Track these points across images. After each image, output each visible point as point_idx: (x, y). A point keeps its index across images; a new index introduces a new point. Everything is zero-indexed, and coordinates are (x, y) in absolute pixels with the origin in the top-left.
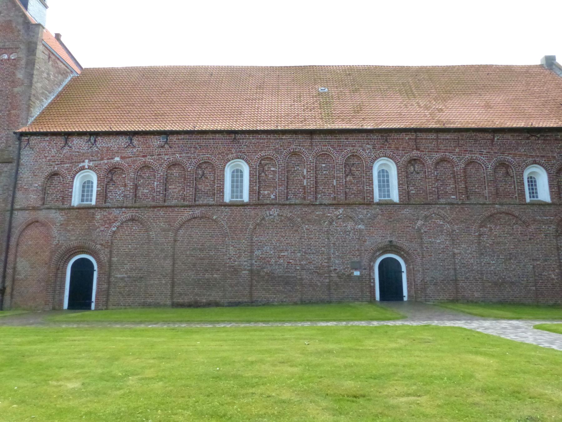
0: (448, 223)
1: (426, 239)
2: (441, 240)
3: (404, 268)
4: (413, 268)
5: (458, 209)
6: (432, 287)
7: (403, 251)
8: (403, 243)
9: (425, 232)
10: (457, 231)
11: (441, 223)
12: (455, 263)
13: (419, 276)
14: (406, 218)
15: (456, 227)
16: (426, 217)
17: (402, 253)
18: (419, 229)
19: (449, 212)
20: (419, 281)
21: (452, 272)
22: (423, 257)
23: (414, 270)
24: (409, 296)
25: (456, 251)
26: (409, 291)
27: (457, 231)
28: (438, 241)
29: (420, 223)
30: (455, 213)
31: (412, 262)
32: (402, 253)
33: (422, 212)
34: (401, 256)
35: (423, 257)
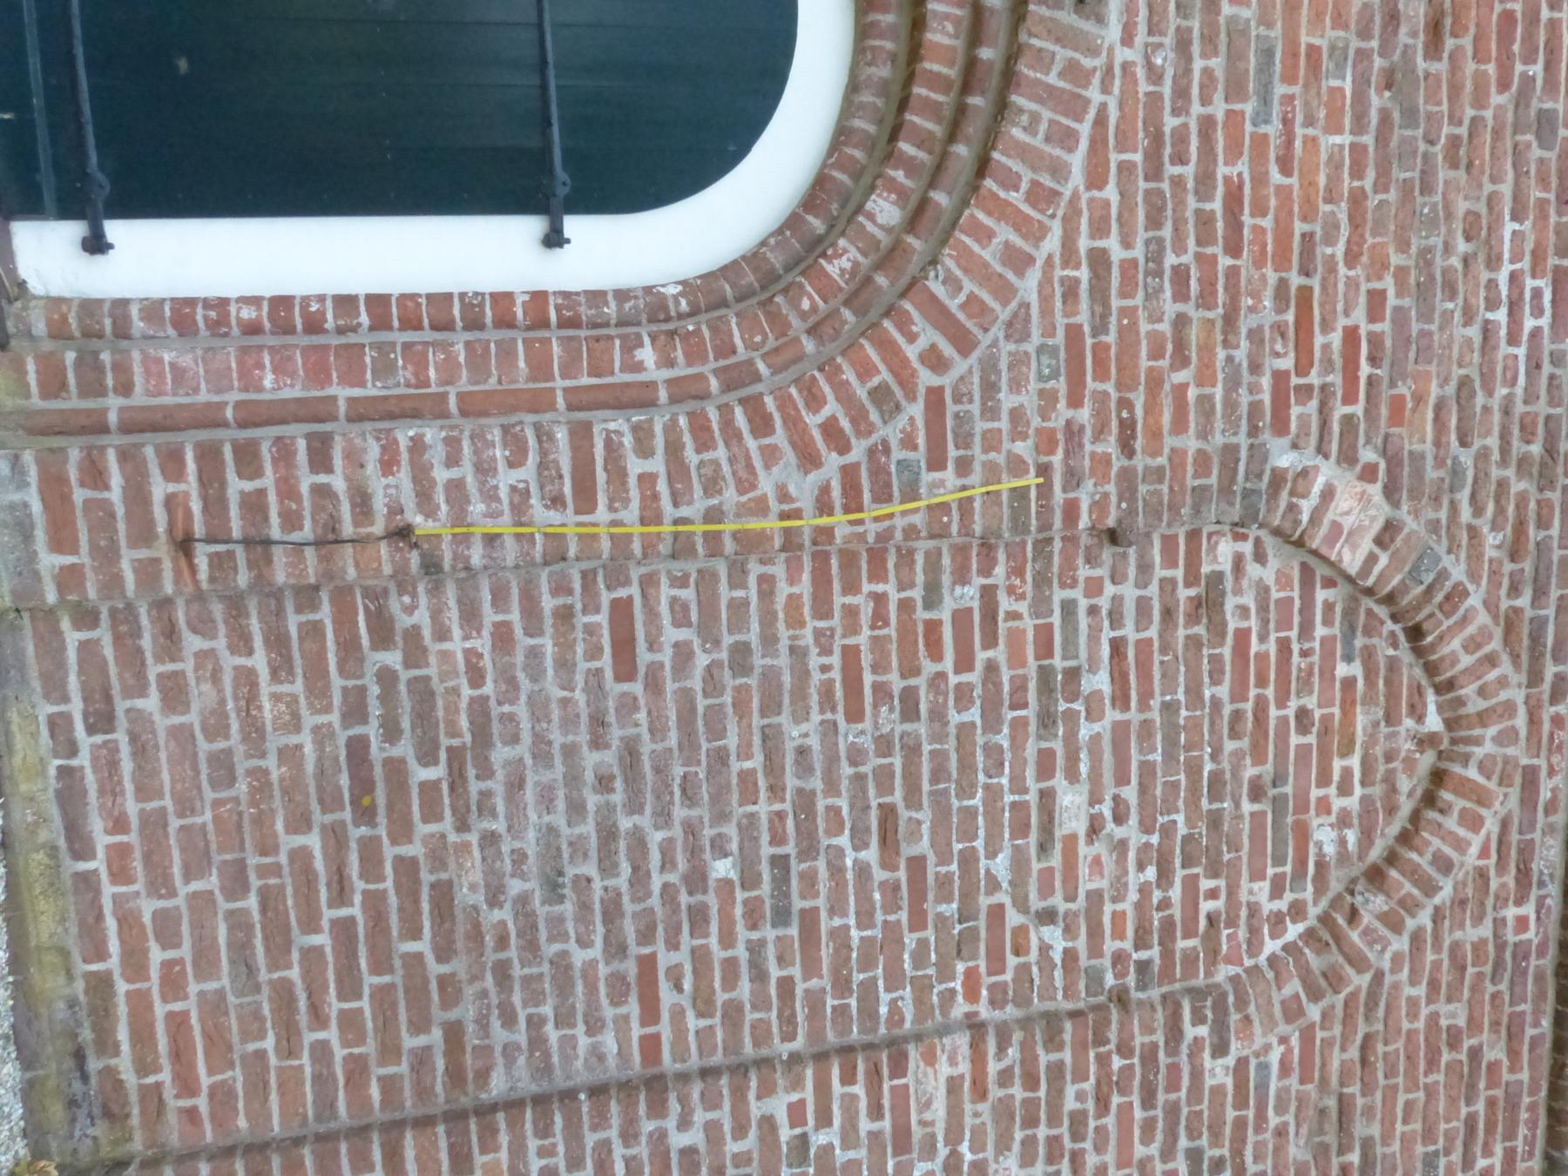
0: (1326, 934)
1: (1118, 597)
2: (1087, 848)
3: (619, 251)
4: (638, 398)
5: (1495, 1052)
6: (314, 735)
7: (918, 214)
8: (1054, 223)
9: (1209, 604)
10: (1218, 1072)
11: (1324, 836)
12: (743, 1071)
13: (494, 492)
14: (1427, 286)
15: (1268, 1044)
16: (1411, 619)
17: (885, 211)
18: (1260, 506)
19: (1472, 933)
20: (391, 490)
21: (605, 1045)
22: (833, 564)
23: (579, 401)
24: (99, 326)
25: (931, 1080)
26: (182, 316)
27: (1218, 1072)
28: (1072, 802)
29: (1351, 509)
30: (1454, 1014)
31: (738, 377)
32: (885, 211)
33: (1492, 541)
34: (828, 200)
35: (833, 564)
